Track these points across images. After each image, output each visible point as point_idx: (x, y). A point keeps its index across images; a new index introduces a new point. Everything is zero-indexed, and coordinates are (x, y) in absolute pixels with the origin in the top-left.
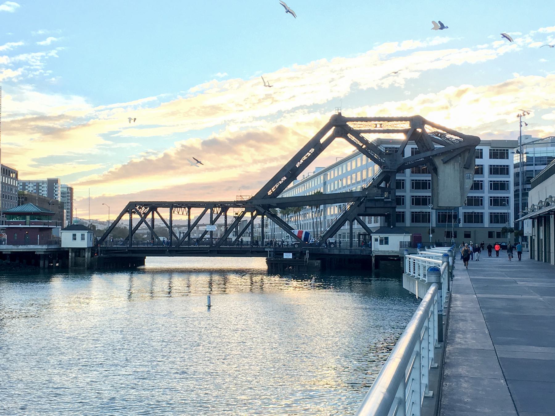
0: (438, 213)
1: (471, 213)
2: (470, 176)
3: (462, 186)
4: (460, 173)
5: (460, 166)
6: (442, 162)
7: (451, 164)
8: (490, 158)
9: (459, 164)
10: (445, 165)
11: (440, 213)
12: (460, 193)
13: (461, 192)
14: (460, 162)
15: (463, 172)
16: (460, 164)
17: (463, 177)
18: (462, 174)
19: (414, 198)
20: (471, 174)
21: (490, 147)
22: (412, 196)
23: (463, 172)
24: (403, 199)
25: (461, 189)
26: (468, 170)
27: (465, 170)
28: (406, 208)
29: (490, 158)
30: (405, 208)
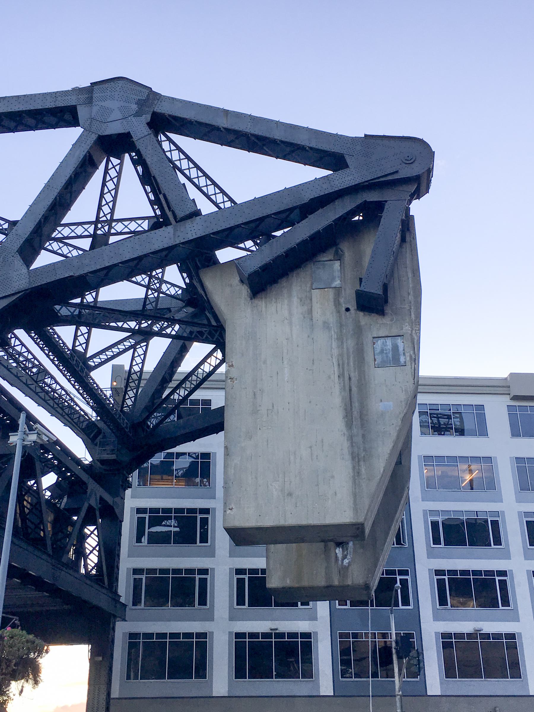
0: (341, 635)
1: (469, 635)
2: (395, 348)
3: (356, 405)
4: (340, 339)
5: (337, 303)
6: (245, 290)
7: (295, 300)
8: (515, 433)
9: (331, 294)
10: (261, 303)
11: (347, 635)
12: (346, 444)
13: (351, 438)
14: (337, 283)
15: (359, 331)
16: (338, 291)
17: (360, 352)
18: (350, 343)
19: (246, 577)
20: (399, 341)
21: (507, 398)
22: (239, 571)
23: (359, 331)
24: (203, 582)
25: (349, 425)
26: (386, 320)
27: (364, 319)
28: (212, 620)
29: (515, 433)
30: (211, 618)
